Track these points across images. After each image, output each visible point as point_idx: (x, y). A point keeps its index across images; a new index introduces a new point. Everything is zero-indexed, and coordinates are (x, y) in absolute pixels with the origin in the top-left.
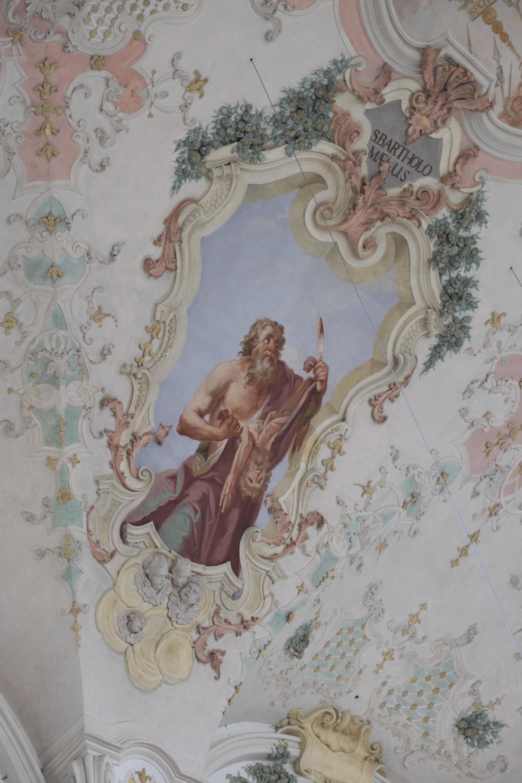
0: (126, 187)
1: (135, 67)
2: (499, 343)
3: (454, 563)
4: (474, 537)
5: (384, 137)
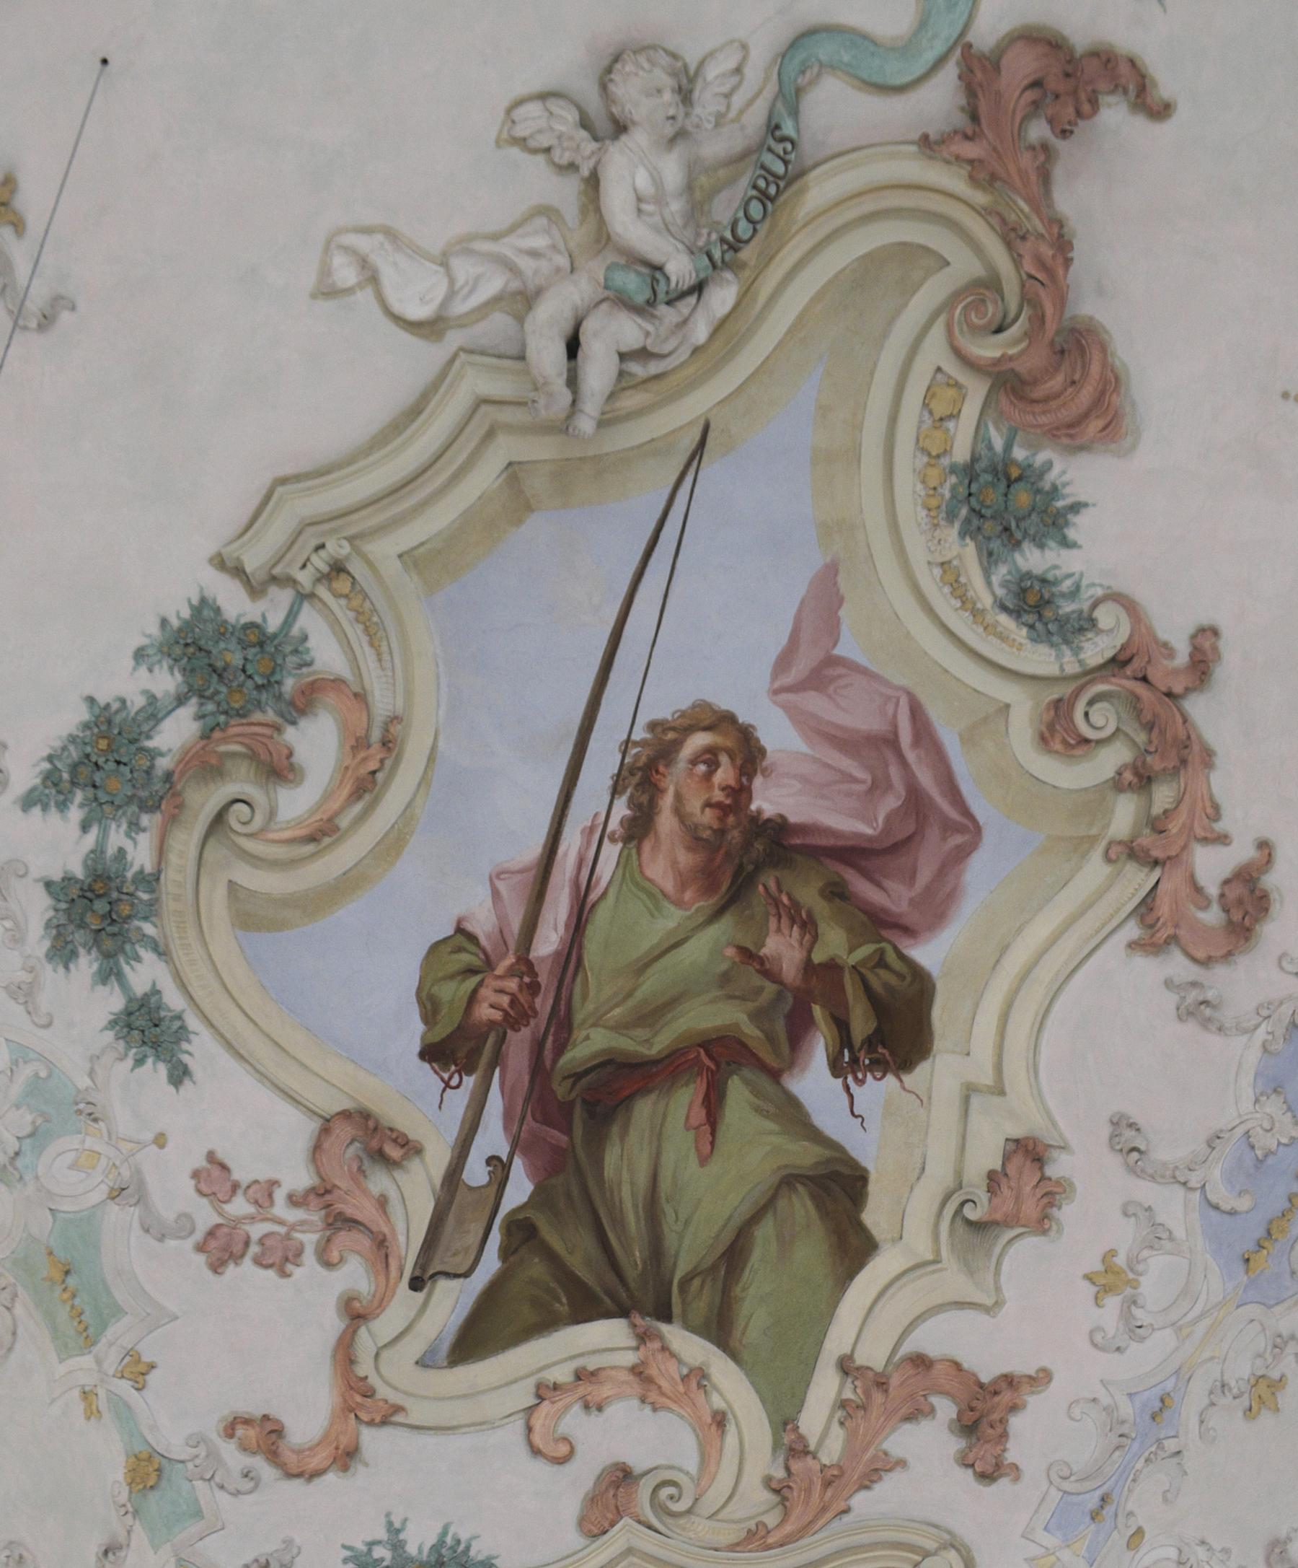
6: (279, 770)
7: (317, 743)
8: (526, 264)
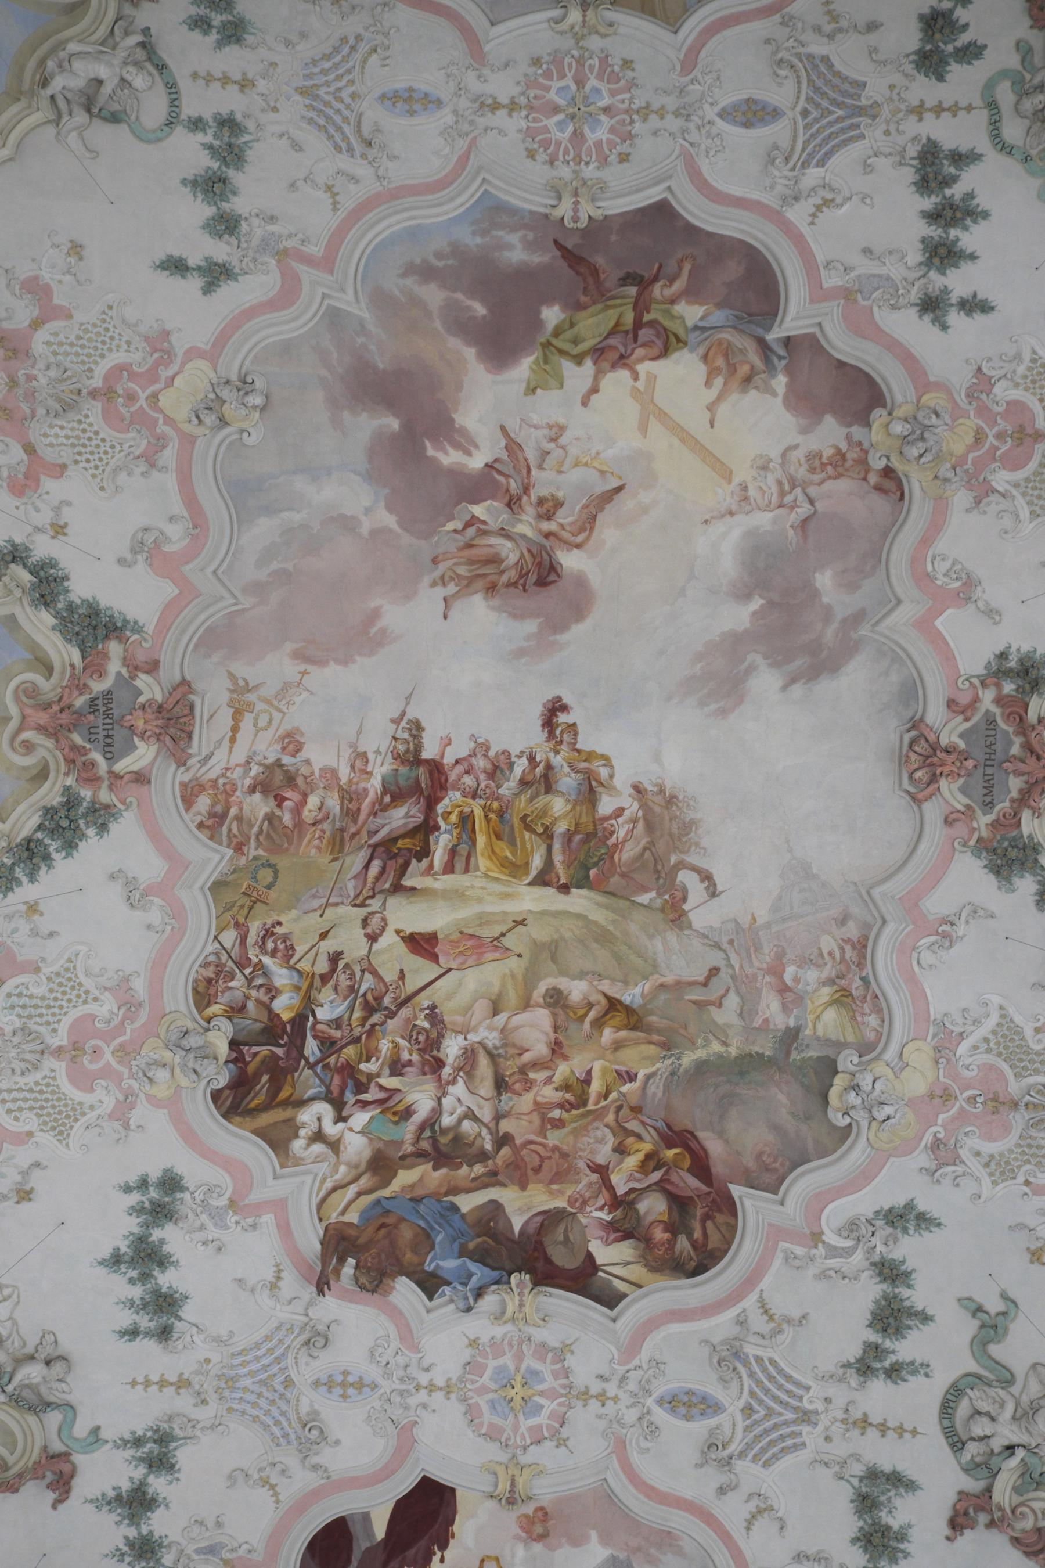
1: (43, 478)
2: (15, 930)
5: (110, 701)
8: (10, 1341)
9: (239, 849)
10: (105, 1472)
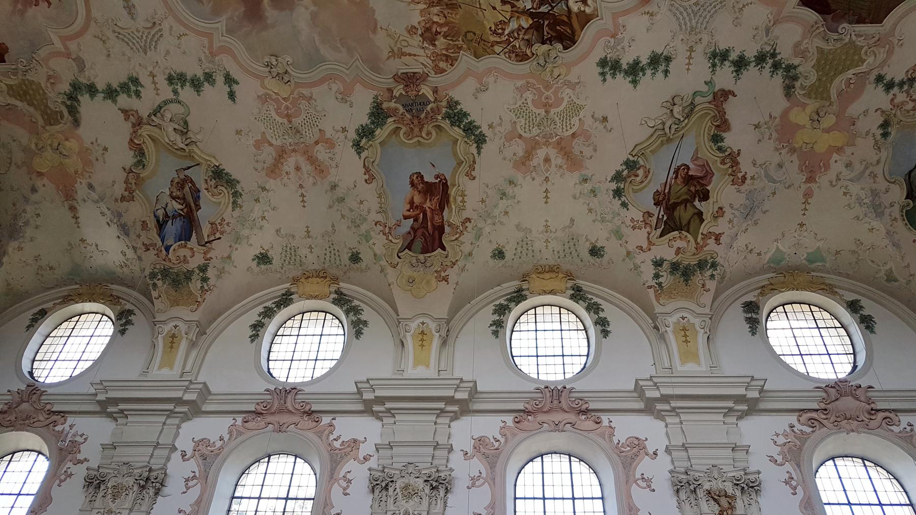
0: (348, 166)
3: (546, 202)
4: (546, 191)
6: (637, 176)
7: (641, 172)
9: (460, 48)
10: (724, 77)
